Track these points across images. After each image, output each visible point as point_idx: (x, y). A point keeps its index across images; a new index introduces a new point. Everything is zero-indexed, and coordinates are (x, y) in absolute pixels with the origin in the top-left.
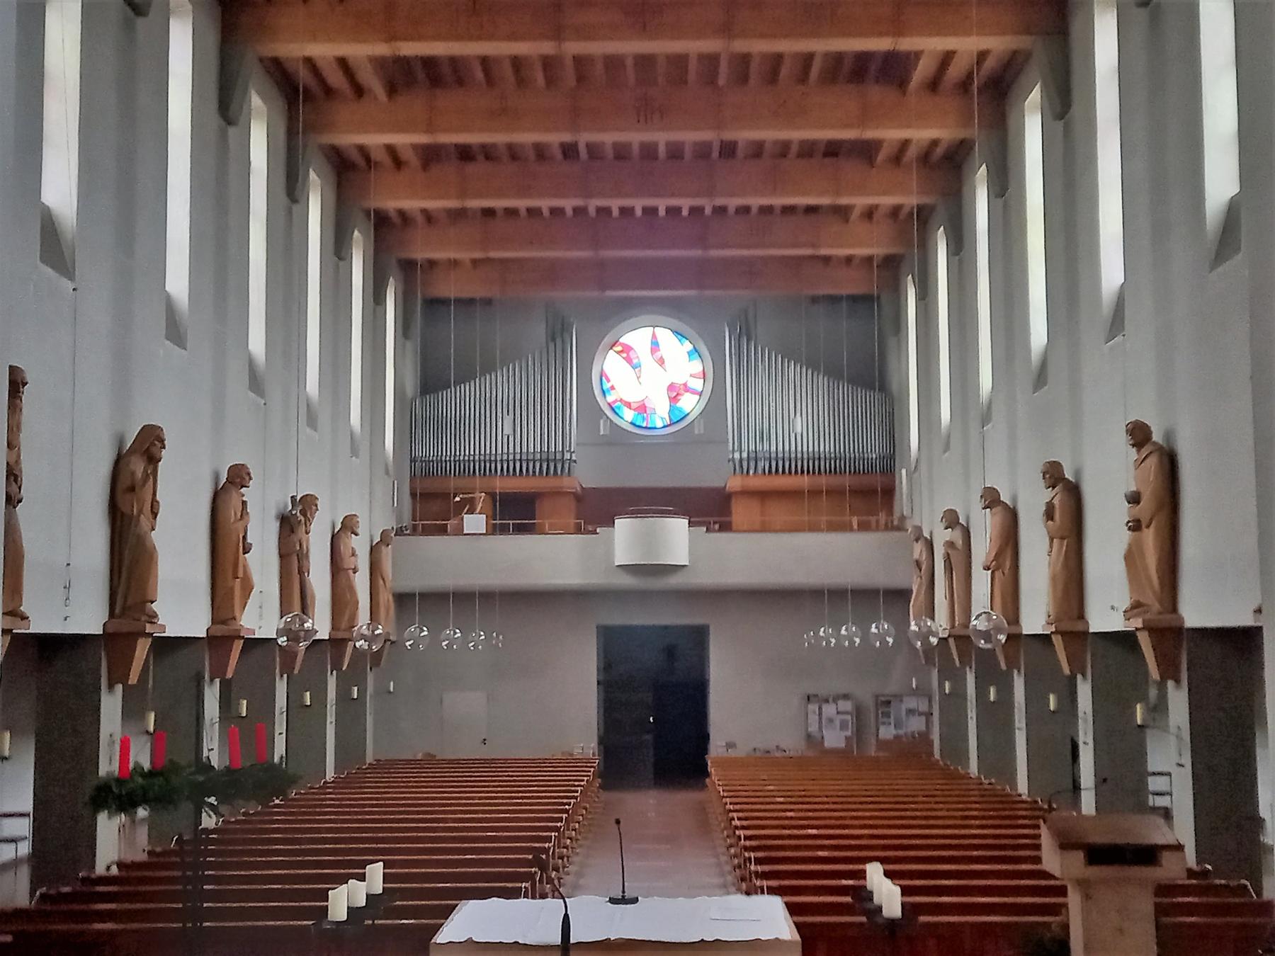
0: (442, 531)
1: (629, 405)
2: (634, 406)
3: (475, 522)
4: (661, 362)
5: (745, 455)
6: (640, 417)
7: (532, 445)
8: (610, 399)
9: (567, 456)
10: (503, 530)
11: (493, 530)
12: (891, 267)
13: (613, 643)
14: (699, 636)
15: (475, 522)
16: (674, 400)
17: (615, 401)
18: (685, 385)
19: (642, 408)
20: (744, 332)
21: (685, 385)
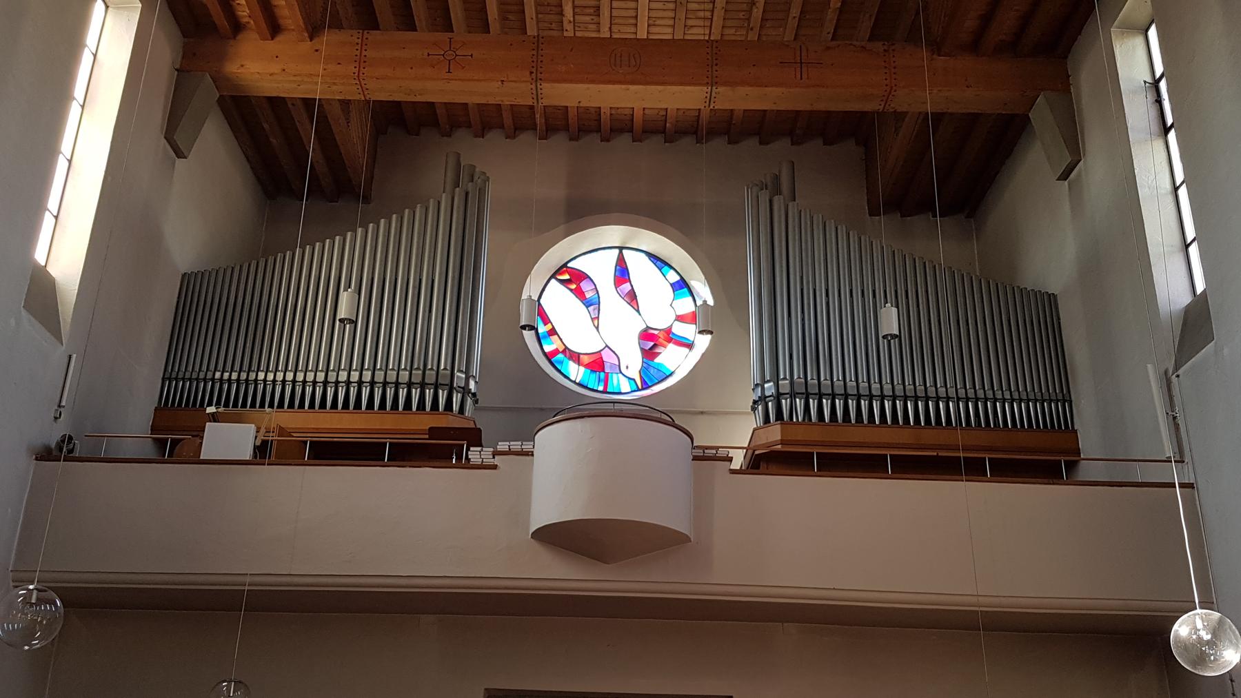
1: (575, 357)
2: (586, 360)
4: (632, 298)
6: (594, 376)
8: (548, 348)
16: (649, 354)
17: (556, 352)
18: (668, 331)
19: (597, 364)
21: (668, 331)
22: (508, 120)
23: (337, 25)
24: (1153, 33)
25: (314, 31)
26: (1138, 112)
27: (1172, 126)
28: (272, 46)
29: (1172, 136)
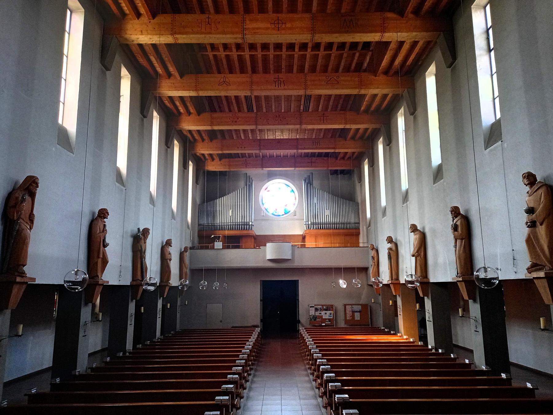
0: (207, 248)
3: (218, 245)
5: (310, 223)
7: (239, 220)
9: (251, 223)
10: (228, 247)
11: (224, 247)
12: (357, 160)
13: (266, 286)
14: (295, 284)
15: (218, 245)
20: (309, 182)
22: (254, 156)
23: (164, 12)
24: (488, 8)
25: (199, 113)
26: (479, 42)
27: (493, 49)
28: (213, 163)
29: (493, 53)
